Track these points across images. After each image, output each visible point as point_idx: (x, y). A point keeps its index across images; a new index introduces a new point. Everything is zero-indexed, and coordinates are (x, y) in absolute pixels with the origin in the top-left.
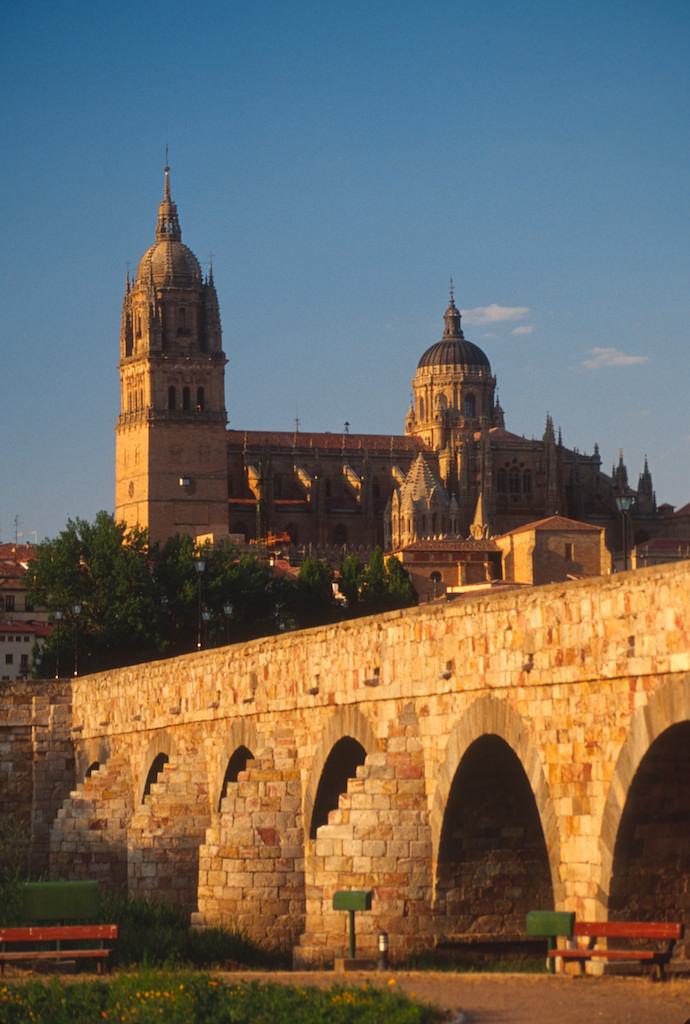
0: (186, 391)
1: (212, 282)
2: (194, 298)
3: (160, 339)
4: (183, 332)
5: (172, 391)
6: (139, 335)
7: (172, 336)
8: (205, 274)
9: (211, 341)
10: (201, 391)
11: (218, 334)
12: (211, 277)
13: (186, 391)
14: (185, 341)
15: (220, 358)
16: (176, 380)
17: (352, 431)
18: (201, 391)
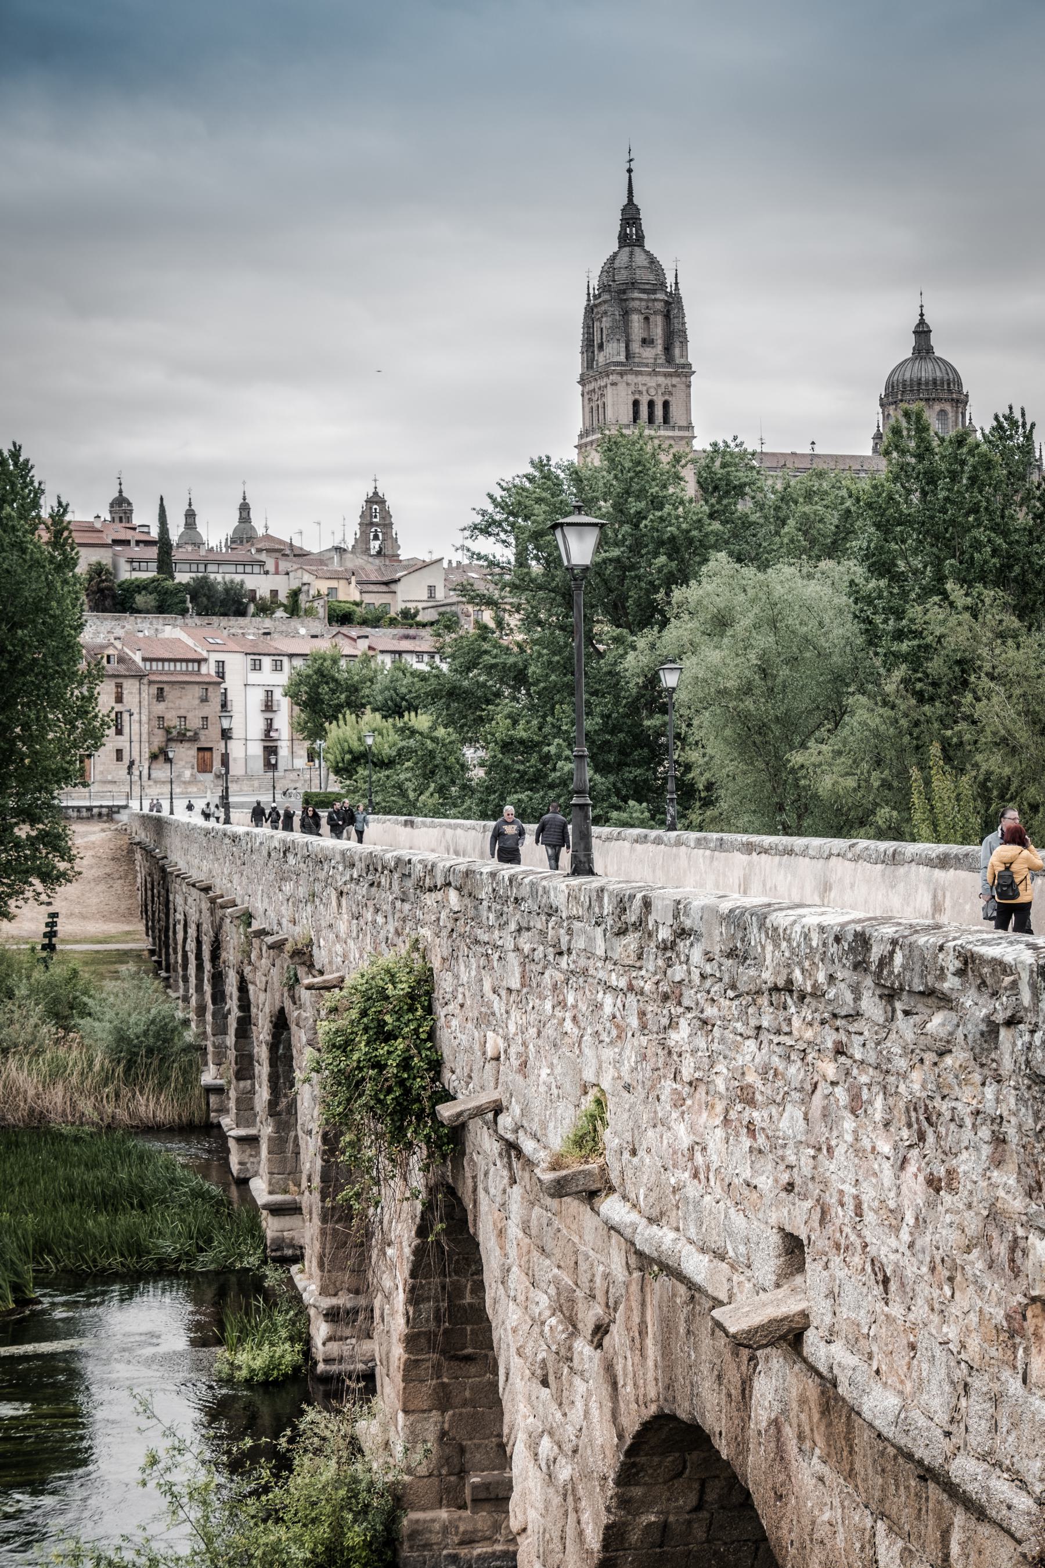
0: (651, 404)
1: (677, 289)
2: (659, 306)
3: (623, 349)
4: (646, 342)
5: (636, 404)
6: (601, 347)
7: (636, 347)
8: (670, 280)
9: (677, 352)
10: (666, 405)
11: (684, 342)
12: (676, 283)
13: (651, 404)
14: (648, 354)
15: (685, 372)
16: (640, 392)
17: (818, 451)
18: (666, 405)
